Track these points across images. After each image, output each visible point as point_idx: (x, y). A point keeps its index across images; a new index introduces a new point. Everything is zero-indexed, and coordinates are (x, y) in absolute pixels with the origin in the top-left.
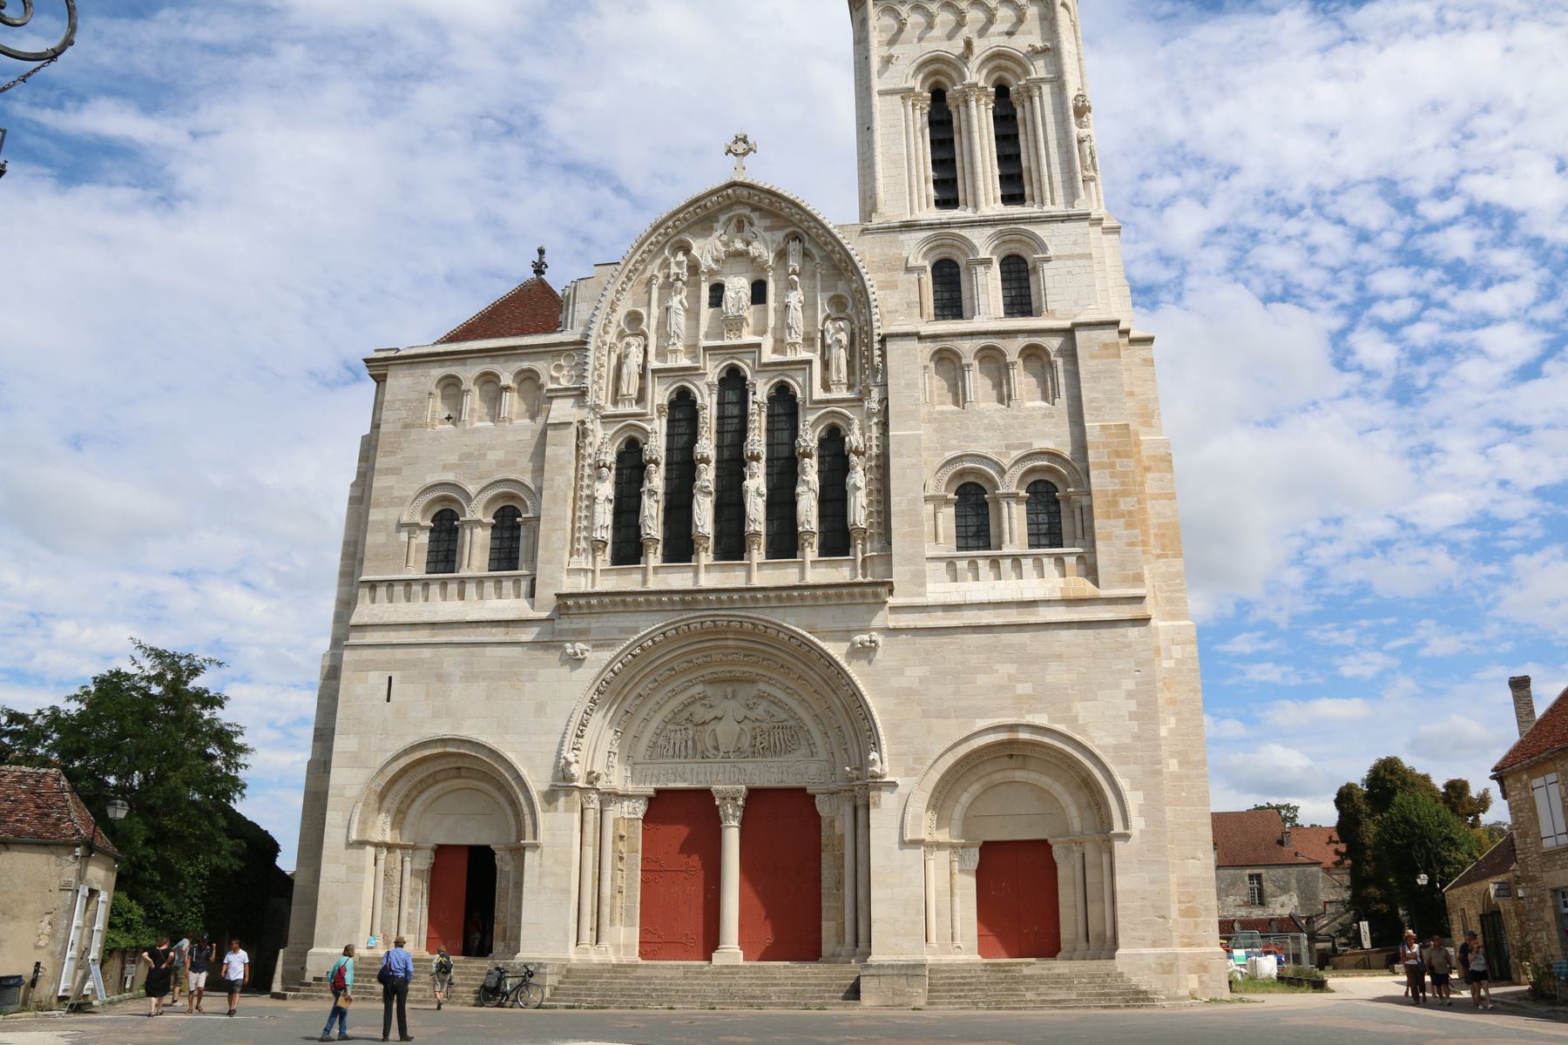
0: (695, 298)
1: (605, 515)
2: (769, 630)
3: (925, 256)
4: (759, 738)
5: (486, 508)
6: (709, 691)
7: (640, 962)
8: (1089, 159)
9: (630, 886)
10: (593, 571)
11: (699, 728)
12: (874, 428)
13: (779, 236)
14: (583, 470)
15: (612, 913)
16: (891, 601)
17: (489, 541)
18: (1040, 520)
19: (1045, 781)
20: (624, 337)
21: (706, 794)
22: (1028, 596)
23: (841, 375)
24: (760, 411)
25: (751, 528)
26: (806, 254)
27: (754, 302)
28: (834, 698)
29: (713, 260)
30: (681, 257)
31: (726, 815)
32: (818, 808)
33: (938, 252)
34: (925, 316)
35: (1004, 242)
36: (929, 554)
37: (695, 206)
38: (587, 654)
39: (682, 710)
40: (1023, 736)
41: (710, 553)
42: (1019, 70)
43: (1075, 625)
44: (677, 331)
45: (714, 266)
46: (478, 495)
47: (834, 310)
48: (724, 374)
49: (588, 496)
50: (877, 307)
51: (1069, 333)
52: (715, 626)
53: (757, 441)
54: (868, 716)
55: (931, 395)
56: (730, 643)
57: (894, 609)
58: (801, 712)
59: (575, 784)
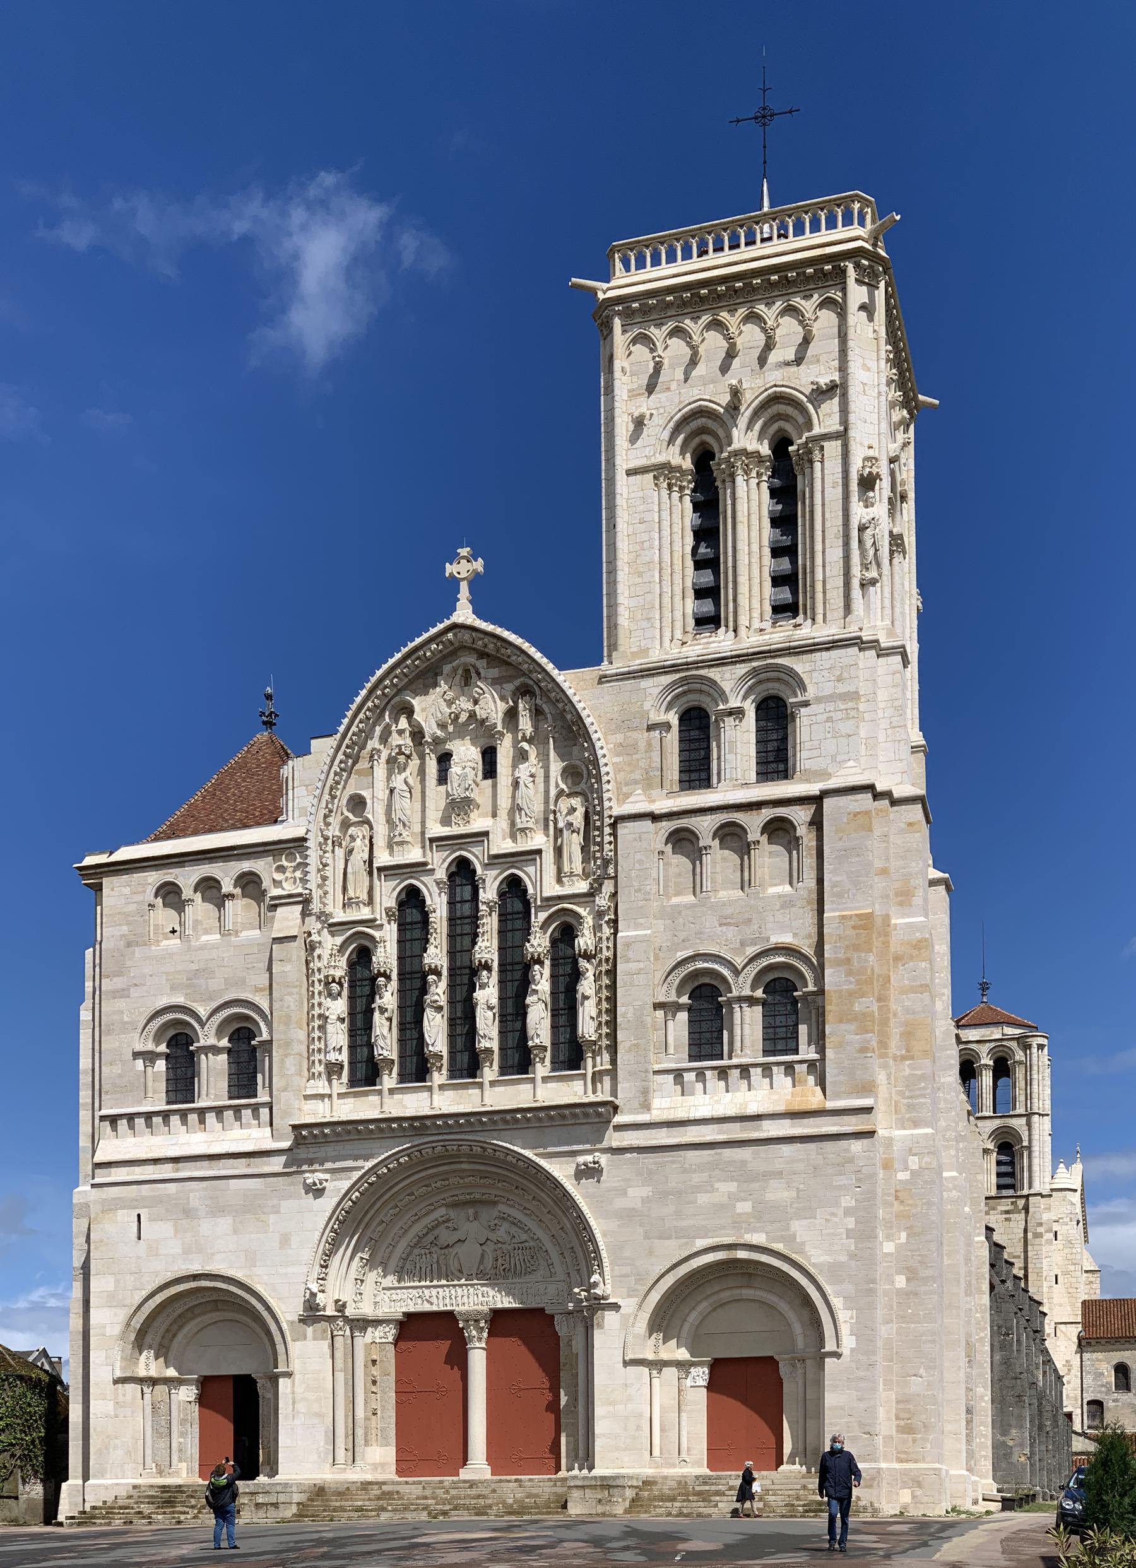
0: (422, 772)
1: (338, 1035)
2: (497, 1153)
3: (668, 709)
4: (500, 1261)
5: (219, 1033)
6: (452, 1214)
7: (398, 1479)
8: (871, 552)
9: (383, 1408)
10: (330, 1096)
11: (443, 1251)
12: (605, 926)
13: (510, 687)
14: (313, 986)
15: (366, 1435)
16: (618, 1119)
17: (226, 1067)
18: (778, 1024)
19: (772, 1299)
20: (349, 826)
21: (448, 1317)
22: (752, 1109)
23: (573, 866)
24: (491, 911)
25: (482, 1044)
26: (537, 713)
27: (485, 777)
28: (565, 1219)
29: (438, 725)
30: (403, 723)
31: (471, 1338)
32: (557, 1328)
33: (684, 699)
34: (667, 784)
35: (760, 682)
36: (657, 1067)
37: (413, 657)
38: (325, 1184)
39: (427, 1233)
40: (742, 1254)
41: (444, 1071)
42: (801, 420)
43: (798, 1140)
44: (403, 818)
45: (439, 733)
46: (208, 1019)
47: (569, 781)
48: (453, 869)
49: (320, 1016)
50: (609, 782)
51: (817, 800)
52: (447, 1150)
53: (487, 948)
54: (592, 1239)
55: (666, 887)
56: (465, 1166)
57: (619, 1128)
58: (540, 1233)
59: (322, 1313)
